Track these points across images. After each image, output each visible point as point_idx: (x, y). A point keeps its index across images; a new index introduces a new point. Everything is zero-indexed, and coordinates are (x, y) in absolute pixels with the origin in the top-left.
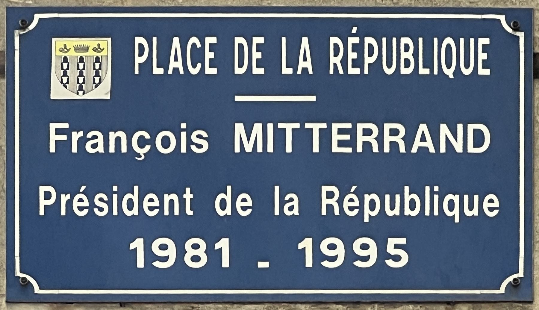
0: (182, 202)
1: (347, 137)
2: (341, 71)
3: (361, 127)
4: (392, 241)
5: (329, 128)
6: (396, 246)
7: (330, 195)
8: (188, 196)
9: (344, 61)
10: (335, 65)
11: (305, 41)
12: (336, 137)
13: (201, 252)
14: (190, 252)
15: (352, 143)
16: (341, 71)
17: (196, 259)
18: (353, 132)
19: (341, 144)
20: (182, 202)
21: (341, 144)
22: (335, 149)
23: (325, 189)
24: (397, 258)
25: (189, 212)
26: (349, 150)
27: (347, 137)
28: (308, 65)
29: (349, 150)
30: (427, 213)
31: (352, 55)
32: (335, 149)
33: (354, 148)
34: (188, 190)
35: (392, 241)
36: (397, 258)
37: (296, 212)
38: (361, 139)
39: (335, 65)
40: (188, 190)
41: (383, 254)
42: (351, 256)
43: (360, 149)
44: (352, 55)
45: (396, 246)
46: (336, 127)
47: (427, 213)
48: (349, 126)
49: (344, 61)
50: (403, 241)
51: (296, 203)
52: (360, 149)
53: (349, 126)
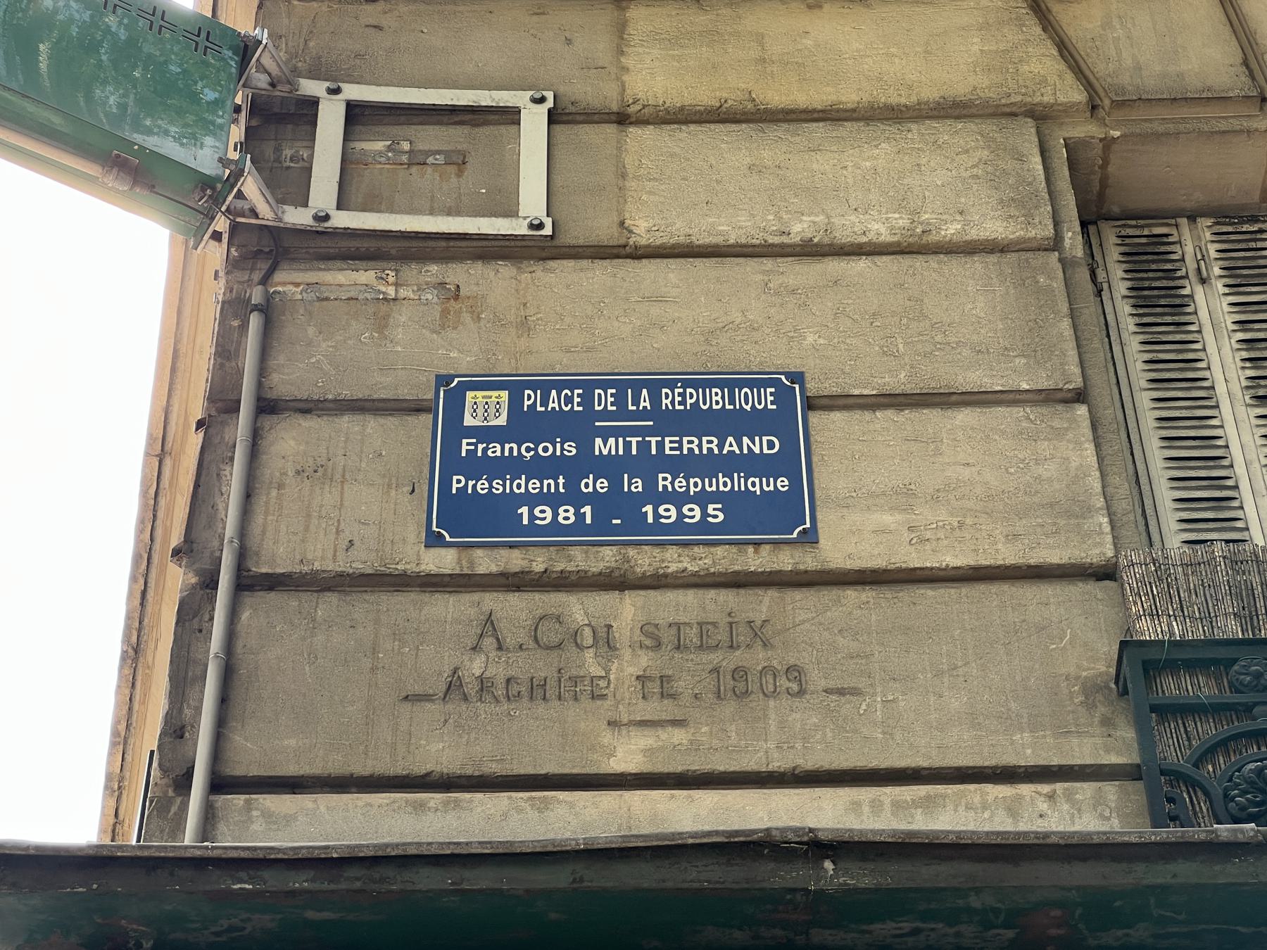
0: (557, 485)
1: (676, 445)
2: (670, 408)
3: (685, 439)
4: (711, 507)
5: (663, 440)
6: (714, 509)
7: (665, 479)
8: (561, 480)
9: (673, 402)
10: (666, 404)
11: (645, 392)
12: (668, 445)
13: (571, 514)
14: (562, 514)
15: (680, 448)
16: (670, 408)
17: (566, 518)
18: (680, 442)
19: (671, 449)
20: (557, 485)
21: (671, 449)
22: (668, 452)
23: (661, 476)
24: (716, 517)
25: (562, 490)
26: (678, 453)
27: (676, 445)
28: (647, 404)
29: (678, 453)
30: (736, 489)
31: (678, 399)
32: (668, 452)
33: (682, 451)
34: (561, 477)
35: (711, 507)
36: (716, 517)
37: (640, 489)
38: (686, 446)
39: (666, 404)
40: (561, 477)
41: (705, 514)
42: (681, 515)
43: (685, 452)
44: (678, 399)
45: (714, 509)
46: (667, 439)
47: (736, 489)
48: (677, 439)
49: (673, 402)
50: (720, 506)
51: (640, 484)
52: (685, 452)
53: (677, 439)
